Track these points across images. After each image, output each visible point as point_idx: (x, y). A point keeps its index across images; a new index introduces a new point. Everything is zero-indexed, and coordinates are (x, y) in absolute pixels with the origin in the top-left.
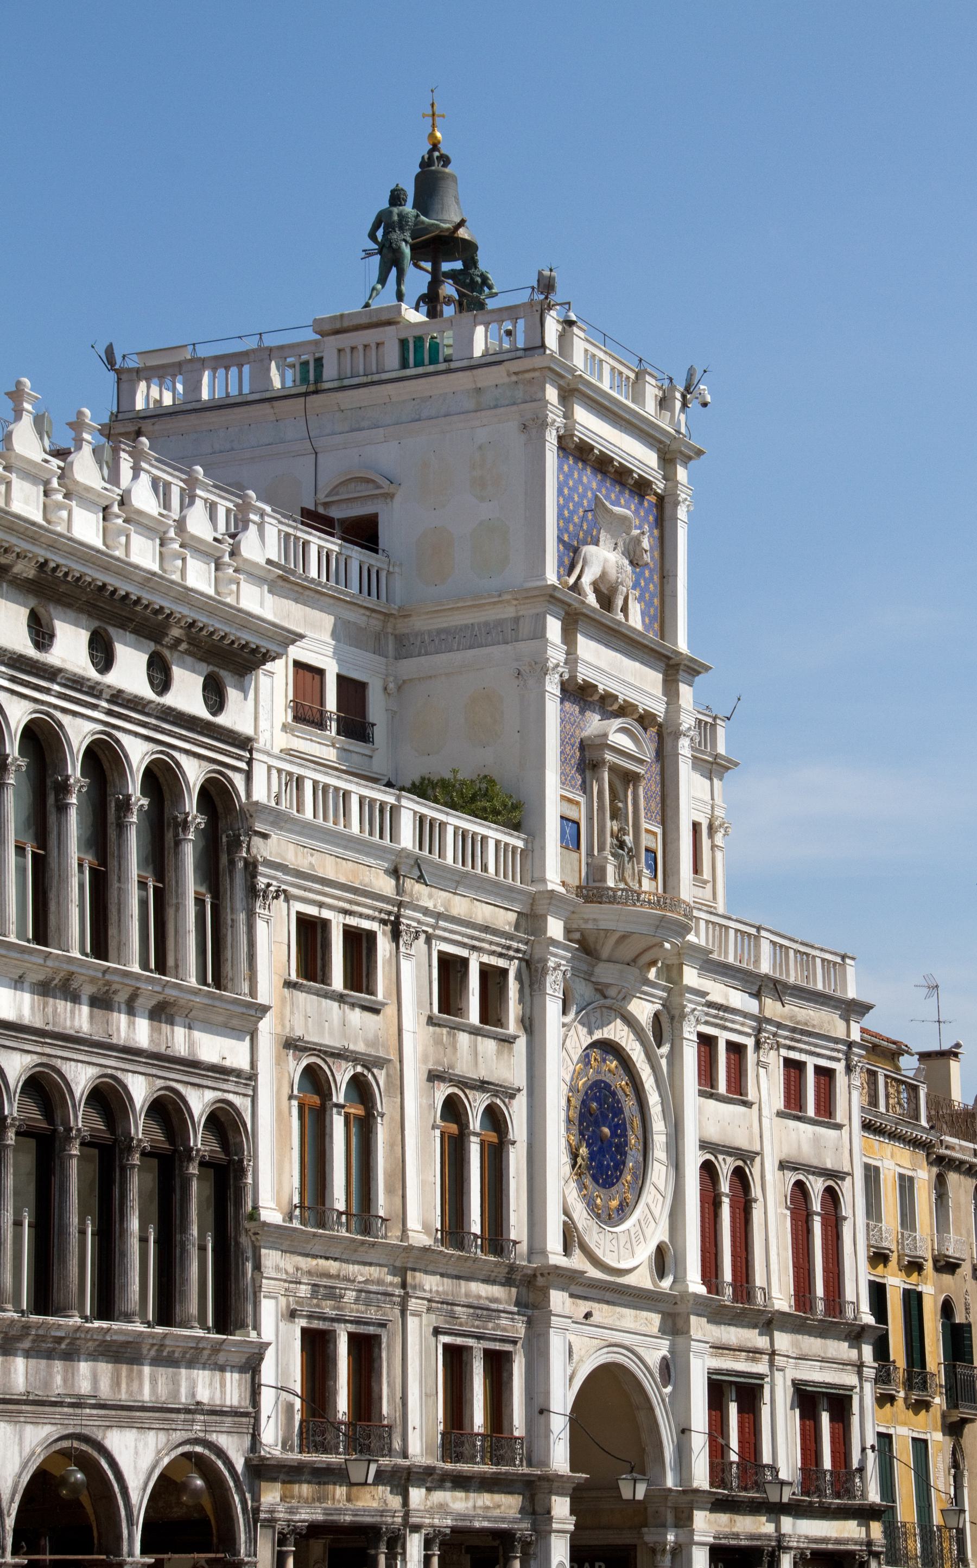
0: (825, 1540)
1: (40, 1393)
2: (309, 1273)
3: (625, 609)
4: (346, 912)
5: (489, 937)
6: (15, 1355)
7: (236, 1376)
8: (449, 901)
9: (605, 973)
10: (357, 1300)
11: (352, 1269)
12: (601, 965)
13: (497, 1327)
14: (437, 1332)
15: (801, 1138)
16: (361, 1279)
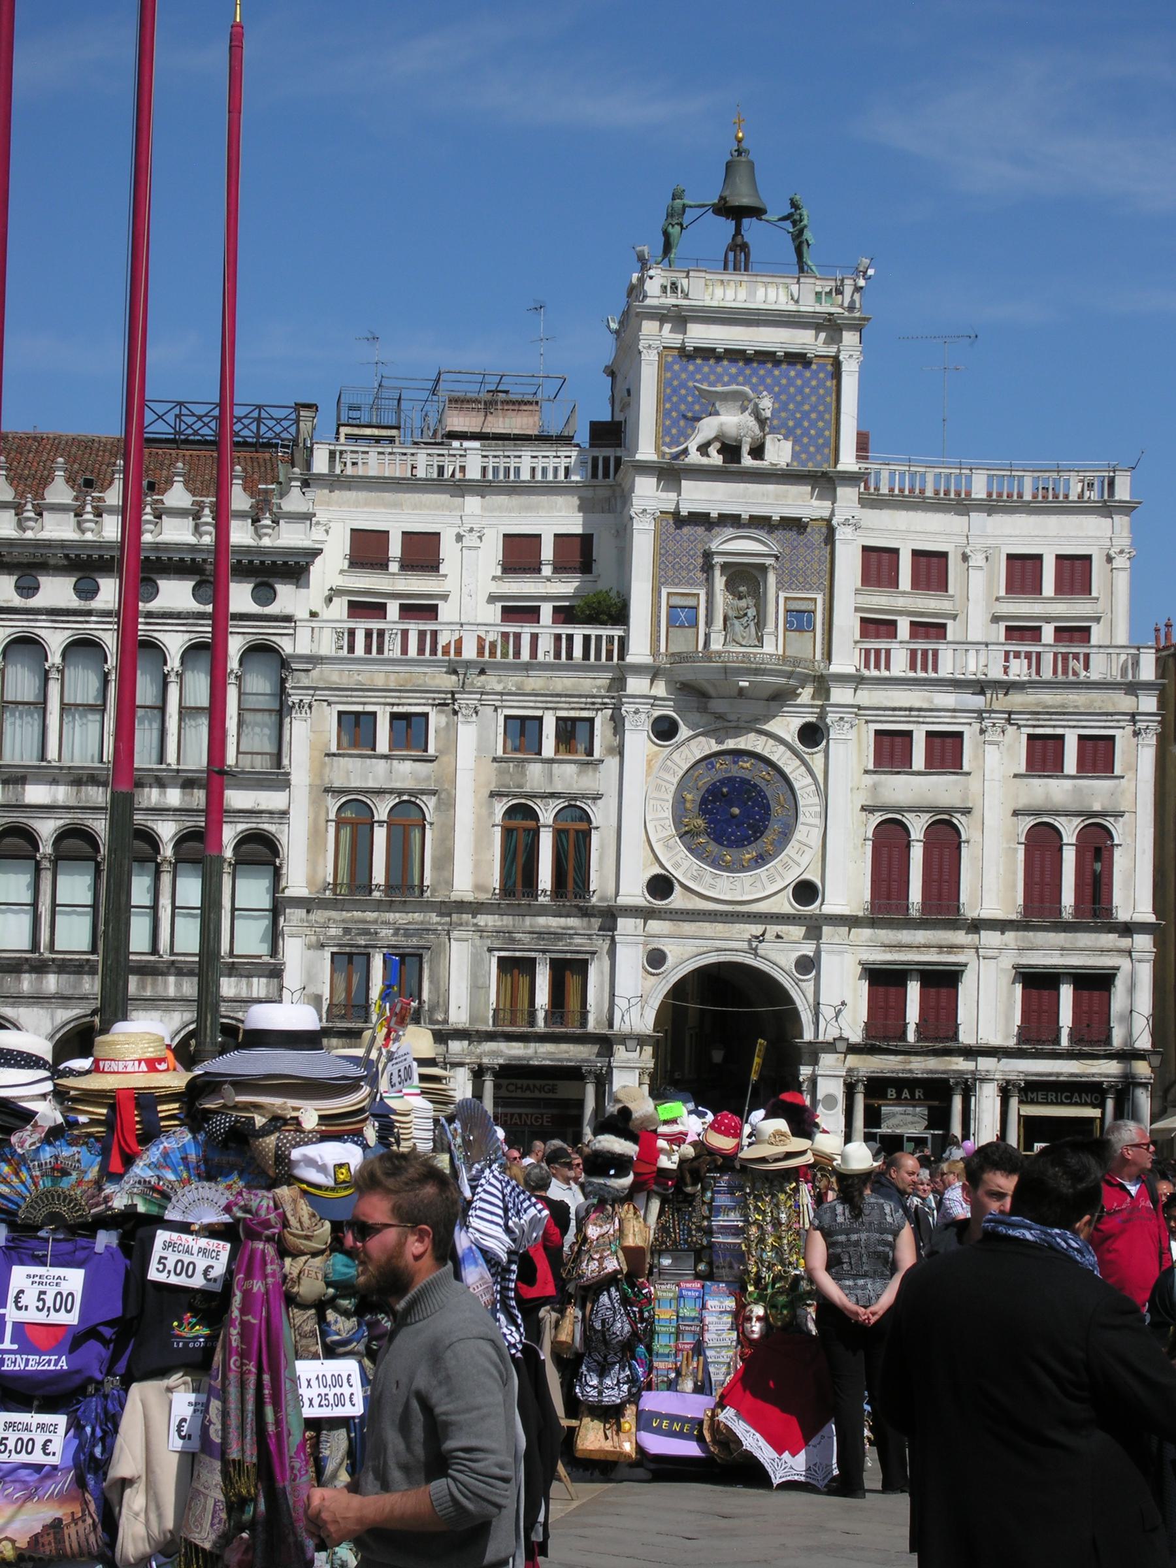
0: (1058, 1075)
1: (68, 992)
2: (343, 921)
3: (758, 452)
4: (393, 705)
5: (563, 699)
6: (47, 972)
7: (263, 980)
8: (522, 682)
9: (717, 705)
10: (395, 934)
11: (391, 916)
13: (570, 944)
14: (490, 950)
15: (1054, 791)
16: (401, 921)
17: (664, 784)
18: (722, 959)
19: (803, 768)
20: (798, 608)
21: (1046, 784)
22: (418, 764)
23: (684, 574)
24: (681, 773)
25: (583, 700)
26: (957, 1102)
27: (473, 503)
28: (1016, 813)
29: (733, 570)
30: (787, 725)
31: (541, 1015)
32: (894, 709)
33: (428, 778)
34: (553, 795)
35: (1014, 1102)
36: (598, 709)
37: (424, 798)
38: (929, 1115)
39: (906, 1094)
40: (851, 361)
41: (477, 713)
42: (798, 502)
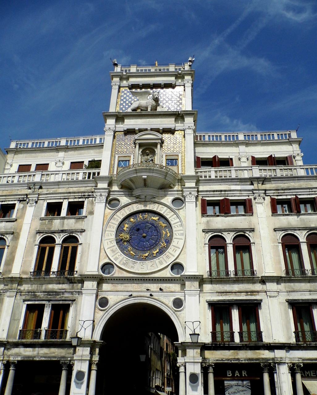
5: (72, 194)
9: (137, 192)
12: (134, 191)
14: (24, 301)
17: (112, 225)
18: (136, 301)
19: (175, 215)
20: (171, 158)
21: (287, 218)
22: (8, 223)
23: (125, 150)
24: (120, 220)
25: (80, 194)
26: (266, 377)
27: (61, 154)
28: (275, 230)
29: (145, 147)
30: (168, 200)
31: (43, 333)
32: (214, 191)
33: (11, 228)
34: (63, 231)
35: (298, 376)
36: (86, 198)
37: (7, 236)
38: (251, 386)
39: (237, 374)
40: (188, 84)
41: (36, 202)
42: (169, 123)
